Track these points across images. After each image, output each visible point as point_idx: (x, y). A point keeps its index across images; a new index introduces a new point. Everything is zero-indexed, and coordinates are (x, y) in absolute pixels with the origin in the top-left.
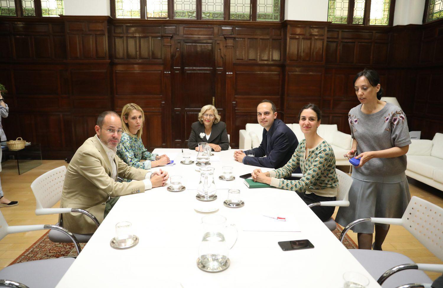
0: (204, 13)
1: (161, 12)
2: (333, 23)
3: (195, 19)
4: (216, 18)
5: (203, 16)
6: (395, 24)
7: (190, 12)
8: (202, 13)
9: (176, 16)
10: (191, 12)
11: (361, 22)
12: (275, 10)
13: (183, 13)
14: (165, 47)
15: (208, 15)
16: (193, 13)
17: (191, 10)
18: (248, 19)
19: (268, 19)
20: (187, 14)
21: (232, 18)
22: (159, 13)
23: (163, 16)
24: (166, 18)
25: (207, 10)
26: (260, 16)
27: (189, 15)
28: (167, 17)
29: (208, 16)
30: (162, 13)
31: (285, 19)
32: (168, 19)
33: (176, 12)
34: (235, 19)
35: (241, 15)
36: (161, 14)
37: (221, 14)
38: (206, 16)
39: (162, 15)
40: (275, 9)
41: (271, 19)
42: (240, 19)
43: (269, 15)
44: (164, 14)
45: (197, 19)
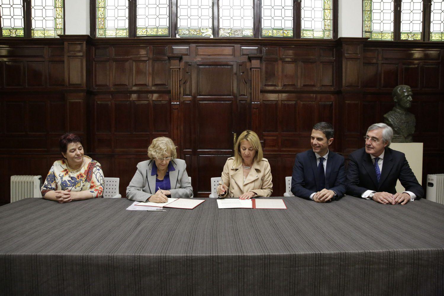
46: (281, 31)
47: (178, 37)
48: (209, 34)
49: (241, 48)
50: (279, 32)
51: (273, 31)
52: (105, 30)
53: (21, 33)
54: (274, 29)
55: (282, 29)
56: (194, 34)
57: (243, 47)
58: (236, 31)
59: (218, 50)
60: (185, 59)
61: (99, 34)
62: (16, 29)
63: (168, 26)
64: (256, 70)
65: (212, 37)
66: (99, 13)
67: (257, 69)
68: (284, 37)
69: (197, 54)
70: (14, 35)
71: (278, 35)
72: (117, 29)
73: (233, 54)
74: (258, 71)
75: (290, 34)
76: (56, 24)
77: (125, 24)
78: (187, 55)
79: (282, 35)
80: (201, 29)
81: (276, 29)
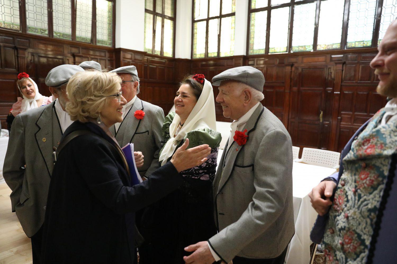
0: (55, 32)
1: (13, 25)
2: (148, 53)
3: (46, 36)
4: (66, 38)
5: (54, 34)
6: (177, 56)
7: (43, 30)
8: (54, 32)
9: (29, 31)
10: (43, 29)
11: (159, 54)
12: (109, 38)
13: (36, 29)
14: (22, 58)
15: (59, 34)
16: (45, 30)
17: (43, 27)
18: (90, 42)
19: (104, 44)
20: (39, 30)
21: (78, 40)
22: (10, 25)
23: (14, 28)
24: (18, 31)
25: (57, 30)
26: (99, 41)
27: (42, 32)
28: (19, 30)
29: (59, 36)
30: (14, 25)
31: (117, 46)
32: (21, 32)
33: (29, 28)
34: (80, 41)
35: (84, 39)
36: (13, 26)
37: (69, 36)
38: (57, 35)
39: (14, 27)
40: (109, 37)
41: (107, 44)
42: (83, 41)
43: (105, 42)
44: (16, 27)
45: (49, 37)
46: (362, 43)
47: (292, 52)
48: (310, 49)
49: (331, 57)
50: (360, 43)
51: (355, 43)
52: (253, 49)
53: (216, 55)
54: (356, 42)
55: (363, 41)
56: (302, 49)
57: (333, 56)
58: (329, 45)
59: (316, 59)
60: (296, 65)
61: (251, 53)
62: (214, 53)
63: (287, 46)
64: (339, 72)
65: (312, 51)
66: (251, 42)
67: (340, 71)
68: (364, 47)
69: (302, 62)
70: (213, 56)
71: (359, 45)
72: (259, 50)
73: (325, 61)
74: (340, 72)
75: (369, 44)
76: (231, 49)
77: (264, 46)
78: (296, 62)
79: (362, 45)
80: (306, 46)
81: (358, 42)
